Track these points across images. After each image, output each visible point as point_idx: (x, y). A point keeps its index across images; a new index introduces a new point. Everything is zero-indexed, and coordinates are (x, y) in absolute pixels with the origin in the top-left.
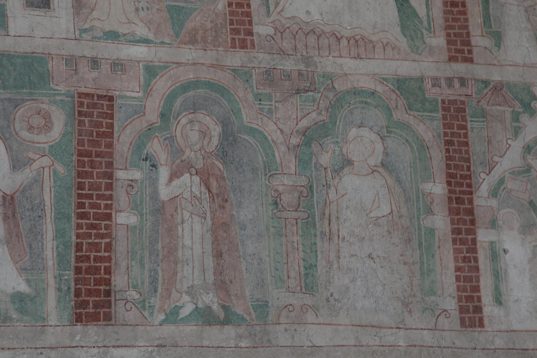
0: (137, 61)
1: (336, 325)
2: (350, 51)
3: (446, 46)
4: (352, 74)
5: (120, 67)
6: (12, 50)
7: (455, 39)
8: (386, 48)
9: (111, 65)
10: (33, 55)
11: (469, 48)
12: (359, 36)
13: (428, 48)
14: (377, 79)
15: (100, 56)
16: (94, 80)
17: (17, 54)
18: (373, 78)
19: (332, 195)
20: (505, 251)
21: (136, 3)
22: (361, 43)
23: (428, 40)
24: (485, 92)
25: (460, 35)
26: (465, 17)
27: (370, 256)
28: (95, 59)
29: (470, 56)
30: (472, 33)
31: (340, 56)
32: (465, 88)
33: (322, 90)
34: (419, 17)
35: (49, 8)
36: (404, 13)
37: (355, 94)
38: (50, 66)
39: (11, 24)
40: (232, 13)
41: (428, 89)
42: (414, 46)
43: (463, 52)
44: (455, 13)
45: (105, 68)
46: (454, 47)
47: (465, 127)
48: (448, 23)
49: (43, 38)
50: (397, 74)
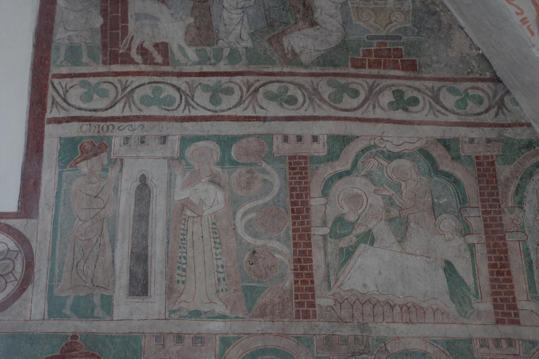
0: (214, 334)
2: (402, 317)
3: (493, 310)
4: (404, 337)
5: (200, 340)
6: (114, 332)
7: (502, 303)
8: (435, 313)
9: (193, 339)
10: (130, 334)
11: (515, 311)
12: (411, 304)
13: (475, 312)
14: (428, 341)
15: (184, 332)
16: (178, 352)
17: (117, 335)
18: (424, 340)
21: (217, 286)
22: (413, 309)
23: (475, 306)
24: (533, 351)
25: (506, 300)
26: (510, 284)
28: (180, 335)
29: (516, 319)
30: (518, 298)
31: (394, 322)
32: (512, 348)
33: (375, 353)
34: (467, 286)
35: (147, 295)
36: (453, 282)
37: (406, 355)
38: (143, 342)
39: (115, 311)
40: (297, 289)
41: (476, 350)
42: (463, 310)
43: (509, 315)
44: (501, 281)
45: (188, 341)
46: (501, 311)
48: (494, 290)
49: (139, 320)
50: (447, 336)
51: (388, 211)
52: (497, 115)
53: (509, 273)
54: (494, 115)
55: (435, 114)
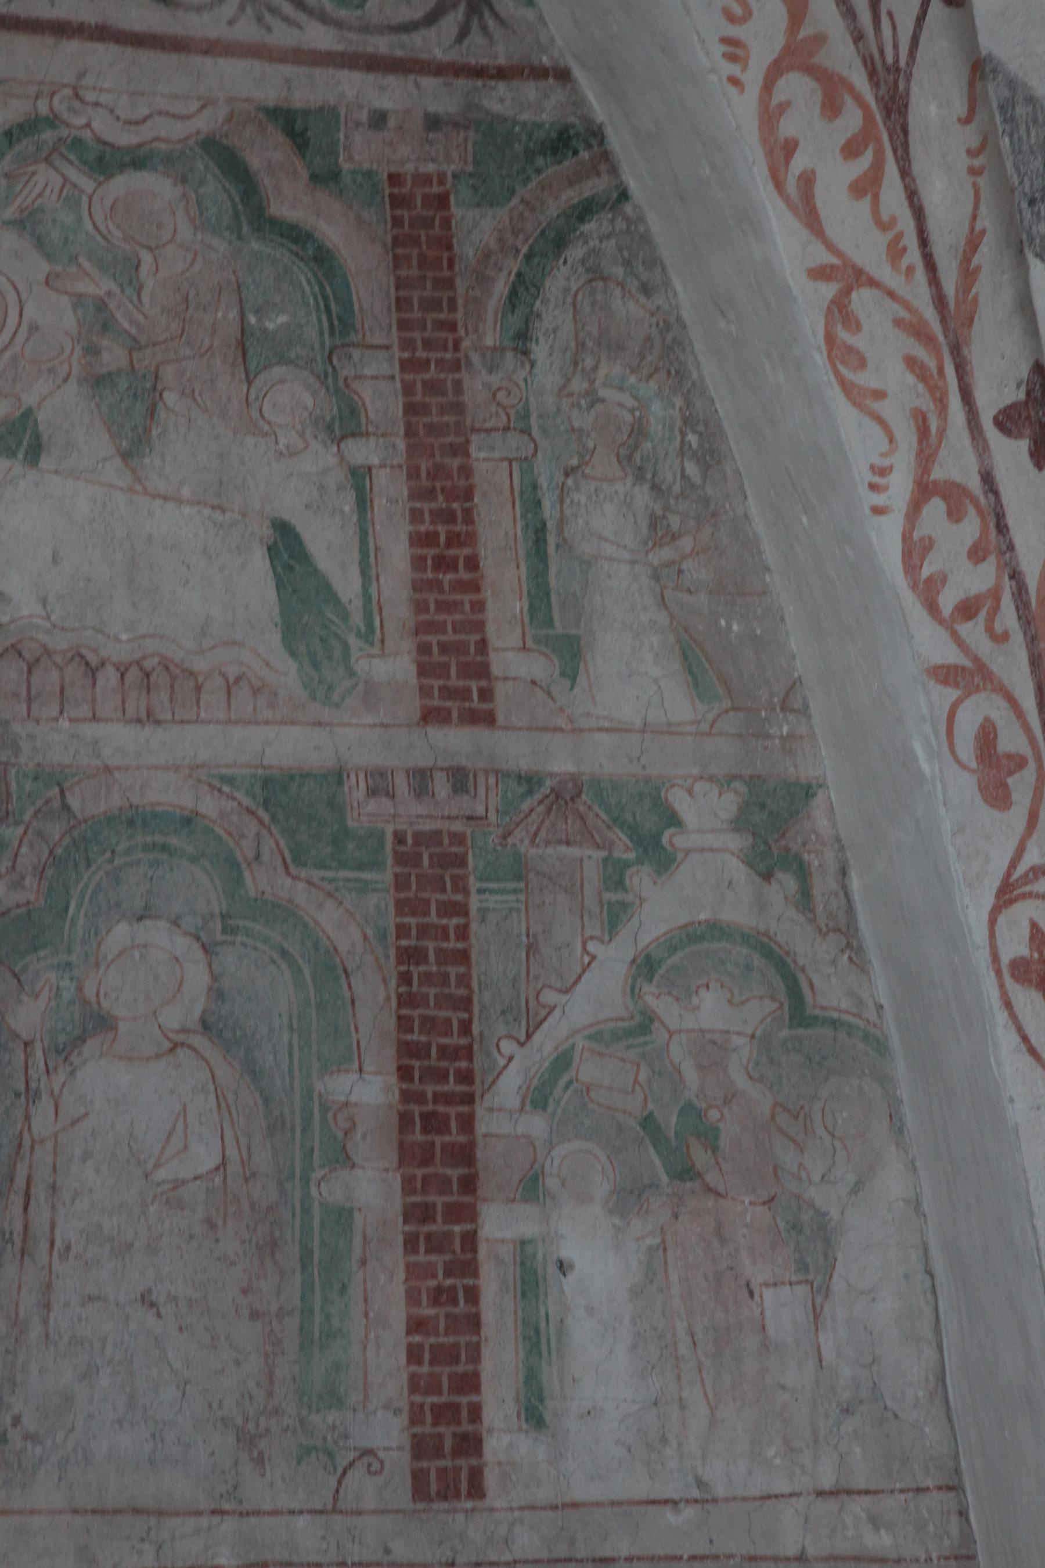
1: (21, 1512)
2: (124, 702)
3: (415, 681)
4: (127, 769)
7: (445, 658)
8: (233, 690)
11: (484, 683)
12: (156, 660)
13: (361, 687)
14: (204, 778)
18: (190, 776)
19: (42, 1121)
20: (563, 1267)
22: (159, 678)
23: (362, 666)
24: (525, 806)
25: (459, 648)
26: (475, 597)
27: (146, 1300)
29: (485, 706)
30: (494, 641)
31: (94, 718)
32: (466, 798)
33: (27, 816)
34: (338, 601)
36: (294, 591)
37: (131, 823)
41: (355, 804)
42: (320, 682)
43: (464, 694)
44: (446, 587)
46: (441, 682)
47: (462, 910)
48: (422, 617)
50: (265, 762)
51: (92, 351)
52: (463, 34)
53: (473, 563)
54: (454, 32)
55: (260, 19)
